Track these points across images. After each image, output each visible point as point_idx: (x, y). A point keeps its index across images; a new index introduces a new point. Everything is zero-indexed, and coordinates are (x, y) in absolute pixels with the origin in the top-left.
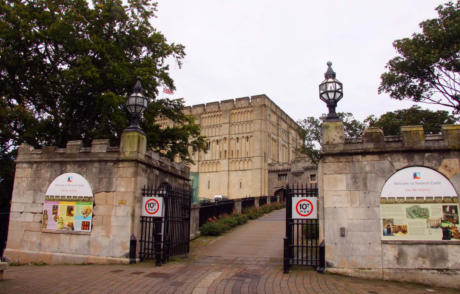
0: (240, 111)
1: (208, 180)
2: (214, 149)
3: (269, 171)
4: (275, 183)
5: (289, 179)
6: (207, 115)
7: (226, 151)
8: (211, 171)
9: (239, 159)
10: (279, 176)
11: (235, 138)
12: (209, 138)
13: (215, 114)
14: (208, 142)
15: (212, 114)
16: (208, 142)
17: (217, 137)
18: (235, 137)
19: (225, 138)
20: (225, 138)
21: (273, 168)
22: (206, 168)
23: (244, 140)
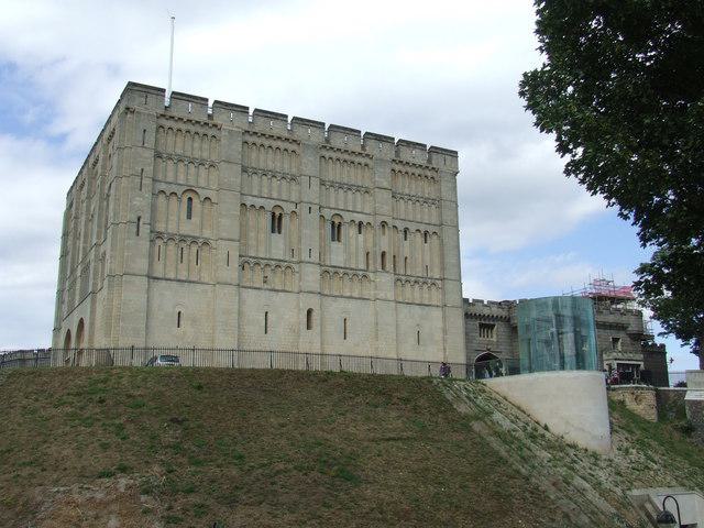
0: (410, 170)
1: (344, 316)
2: (353, 242)
3: (466, 314)
6: (334, 155)
7: (383, 254)
8: (348, 294)
9: (413, 279)
10: (481, 326)
11: (402, 229)
12: (341, 213)
13: (353, 158)
15: (346, 157)
17: (355, 214)
18: (401, 225)
19: (384, 224)
20: (384, 224)
21: (472, 310)
22: (336, 286)
23: (419, 238)
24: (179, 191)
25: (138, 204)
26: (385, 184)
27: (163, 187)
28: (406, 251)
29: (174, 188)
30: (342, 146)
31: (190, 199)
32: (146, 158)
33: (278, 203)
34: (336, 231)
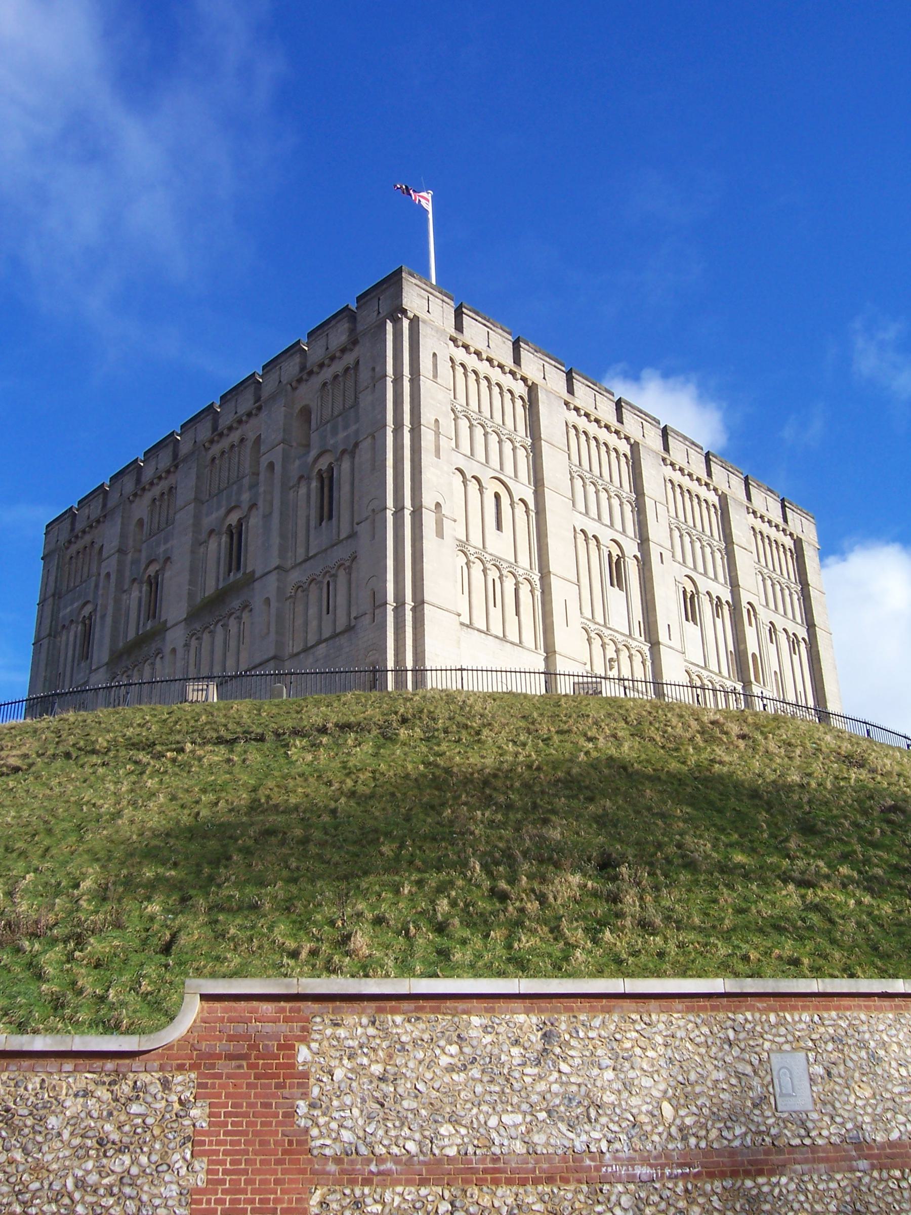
14: (688, 590)
24: (486, 476)
27: (462, 463)
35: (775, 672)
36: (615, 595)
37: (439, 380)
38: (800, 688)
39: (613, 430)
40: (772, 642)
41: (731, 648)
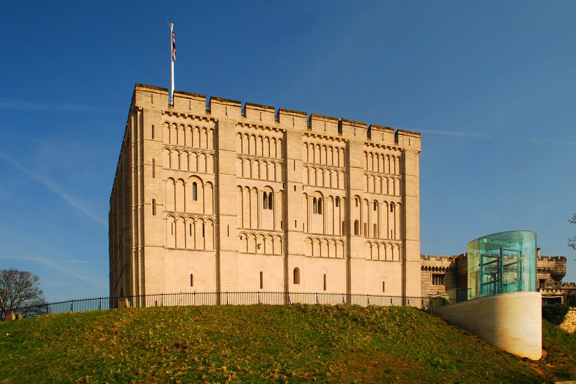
3: (423, 268)
4: (428, 288)
5: (448, 284)
10: (434, 276)
13: (329, 142)
14: (317, 198)
16: (317, 198)
20: (358, 198)
21: (428, 264)
23: (383, 208)
25: (151, 188)
26: (358, 164)
27: (172, 174)
28: (374, 220)
29: (181, 175)
30: (322, 133)
31: (195, 184)
32: (155, 150)
33: (270, 184)
34: (319, 205)
35: (375, 225)
36: (267, 213)
37: (155, 139)
38: (391, 227)
39: (271, 128)
40: (375, 209)
41: (343, 219)
